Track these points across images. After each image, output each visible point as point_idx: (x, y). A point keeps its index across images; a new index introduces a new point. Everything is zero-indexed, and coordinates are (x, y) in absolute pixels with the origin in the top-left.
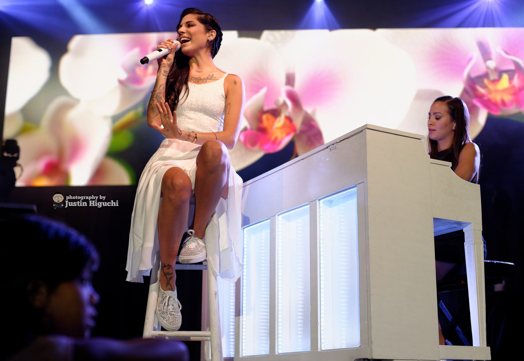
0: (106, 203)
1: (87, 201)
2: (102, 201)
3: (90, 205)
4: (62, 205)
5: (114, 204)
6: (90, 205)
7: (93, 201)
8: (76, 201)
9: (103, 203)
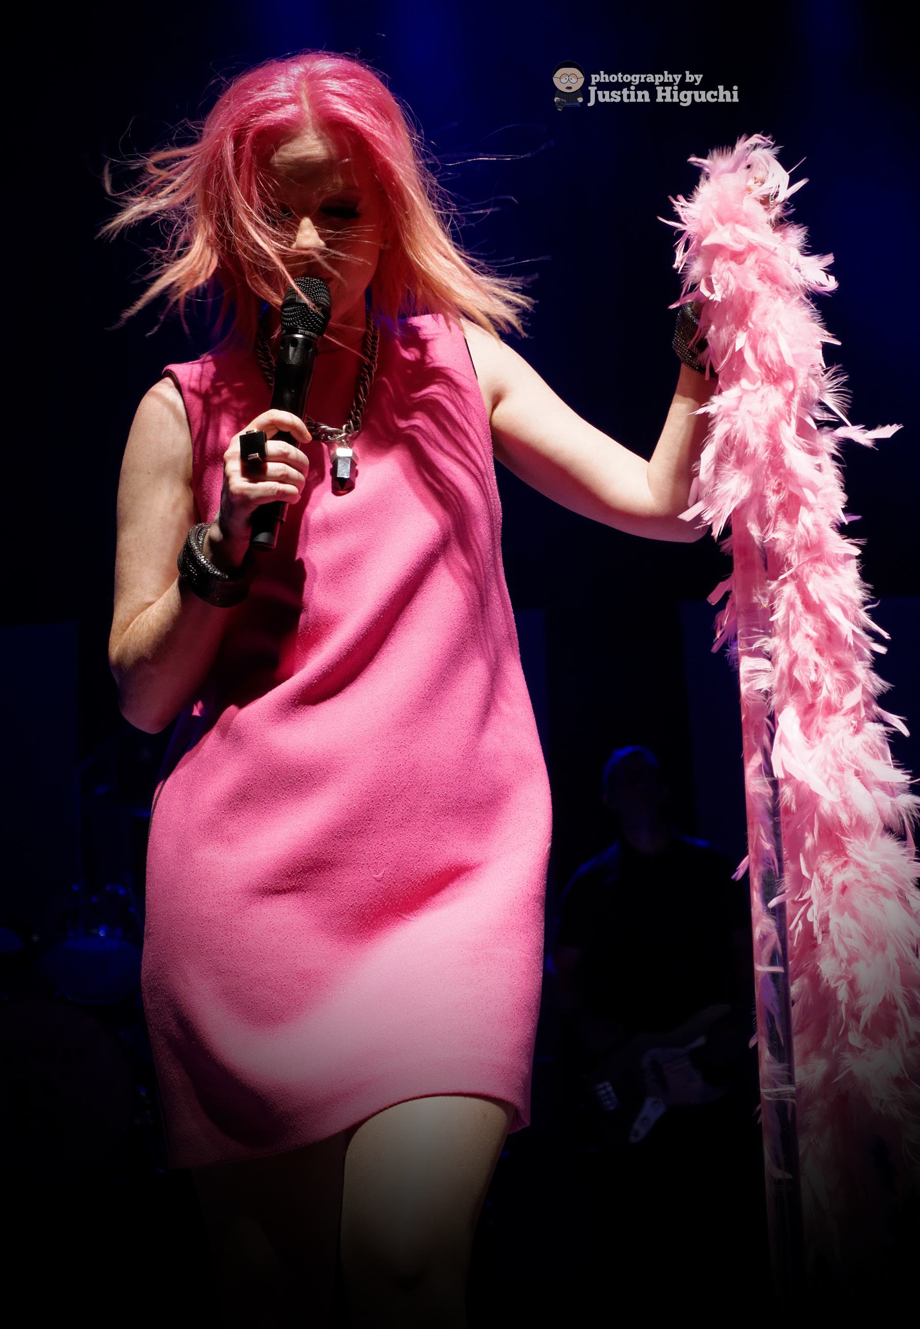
0: (703, 93)
1: (651, 88)
2: (691, 87)
3: (659, 99)
4: (580, 100)
5: (726, 95)
6: (659, 99)
7: (668, 89)
8: (618, 86)
9: (696, 93)
